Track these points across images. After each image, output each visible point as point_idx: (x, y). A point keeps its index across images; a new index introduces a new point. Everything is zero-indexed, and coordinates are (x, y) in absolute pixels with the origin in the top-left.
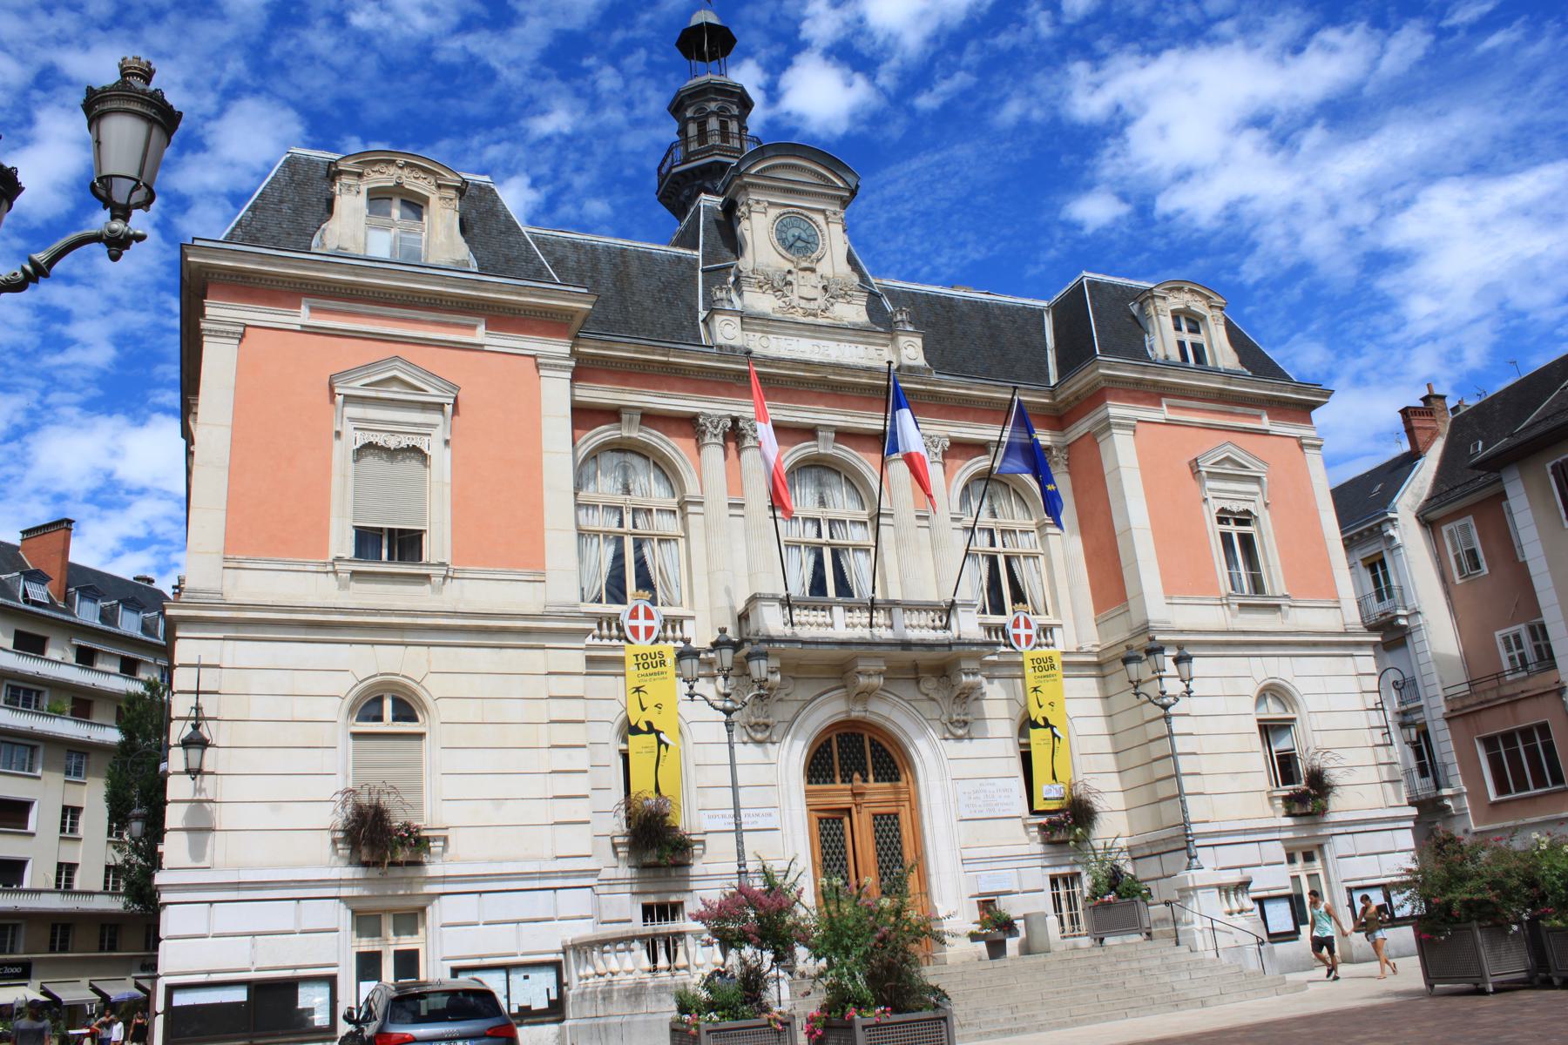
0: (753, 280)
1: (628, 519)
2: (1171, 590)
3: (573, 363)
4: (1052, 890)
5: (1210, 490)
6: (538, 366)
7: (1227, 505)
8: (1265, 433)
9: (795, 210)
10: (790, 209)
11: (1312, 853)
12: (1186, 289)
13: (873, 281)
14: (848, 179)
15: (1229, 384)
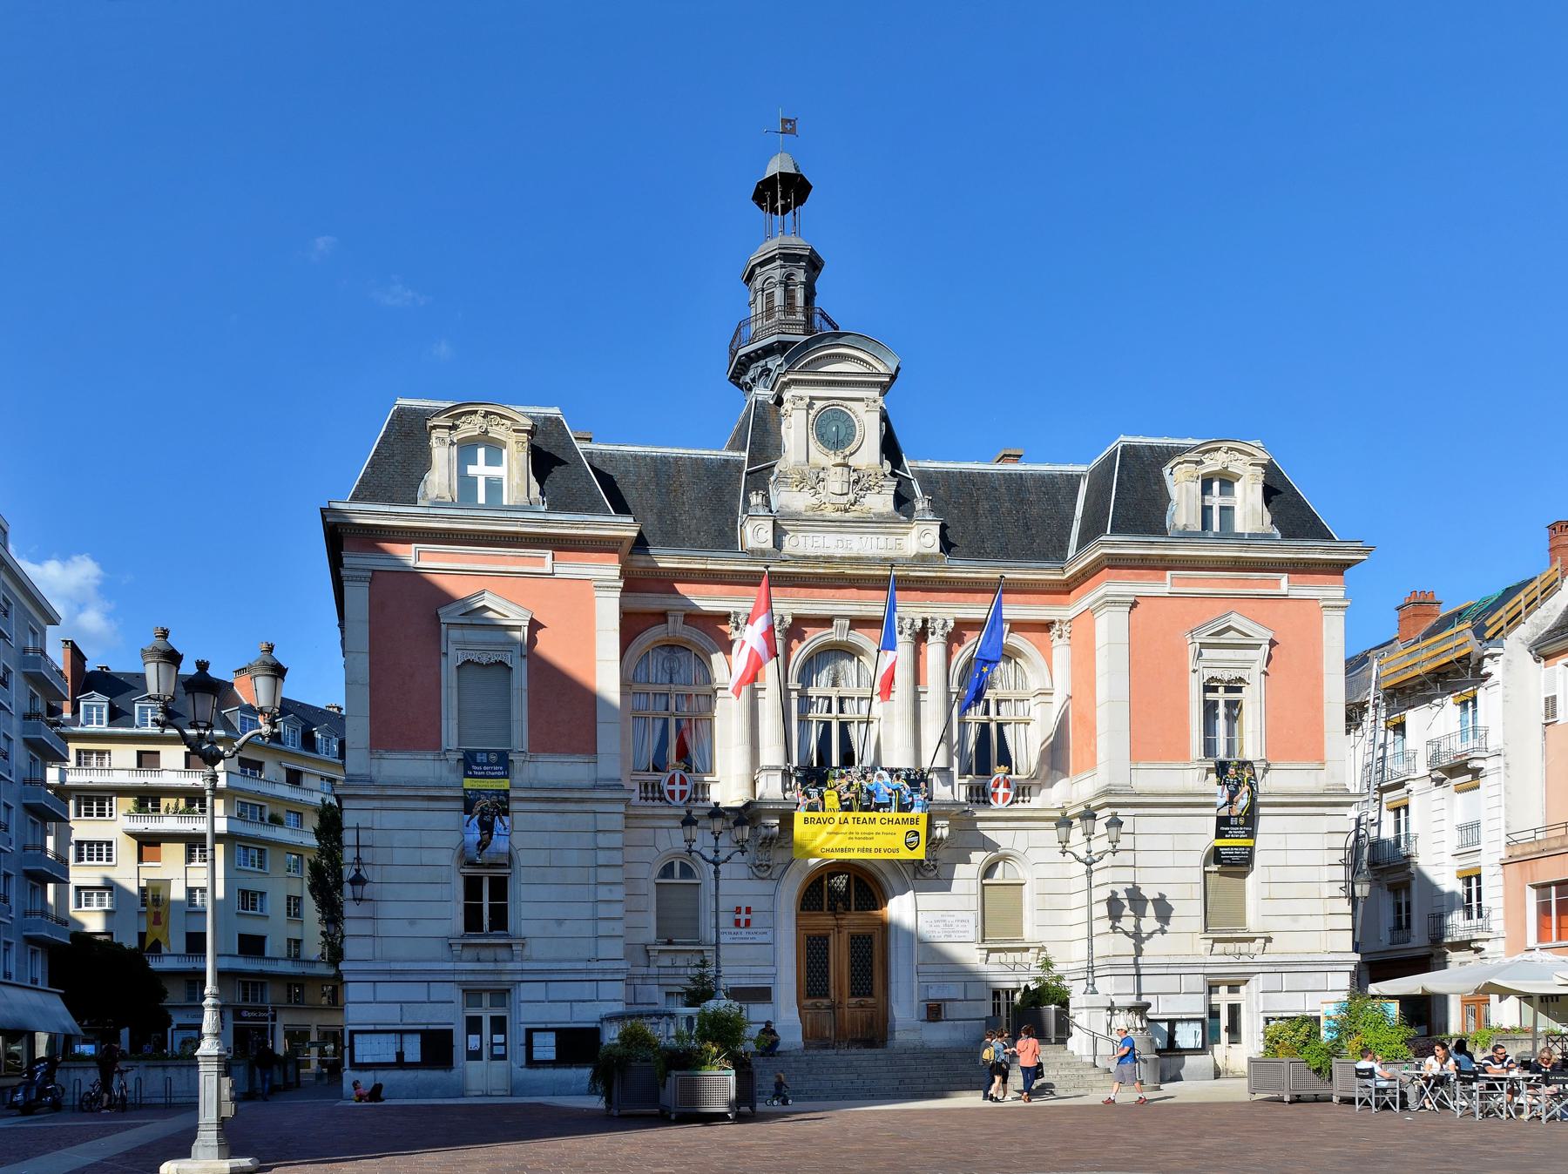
0: (790, 480)
3: (621, 584)
4: (994, 1000)
7: (1217, 674)
8: (1284, 597)
9: (835, 402)
14: (889, 364)
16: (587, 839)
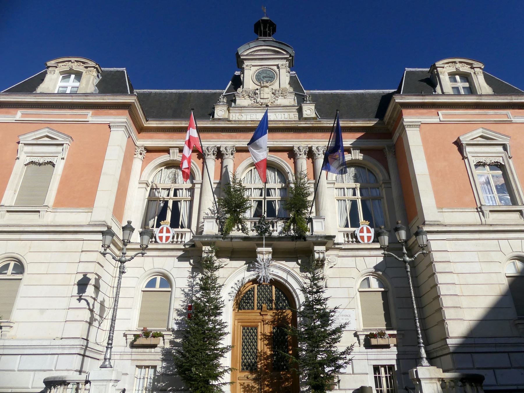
1: (172, 193)
2: (440, 205)
5: (469, 152)
6: (110, 127)
10: (263, 67)
13: (305, 91)
16: (76, 257)
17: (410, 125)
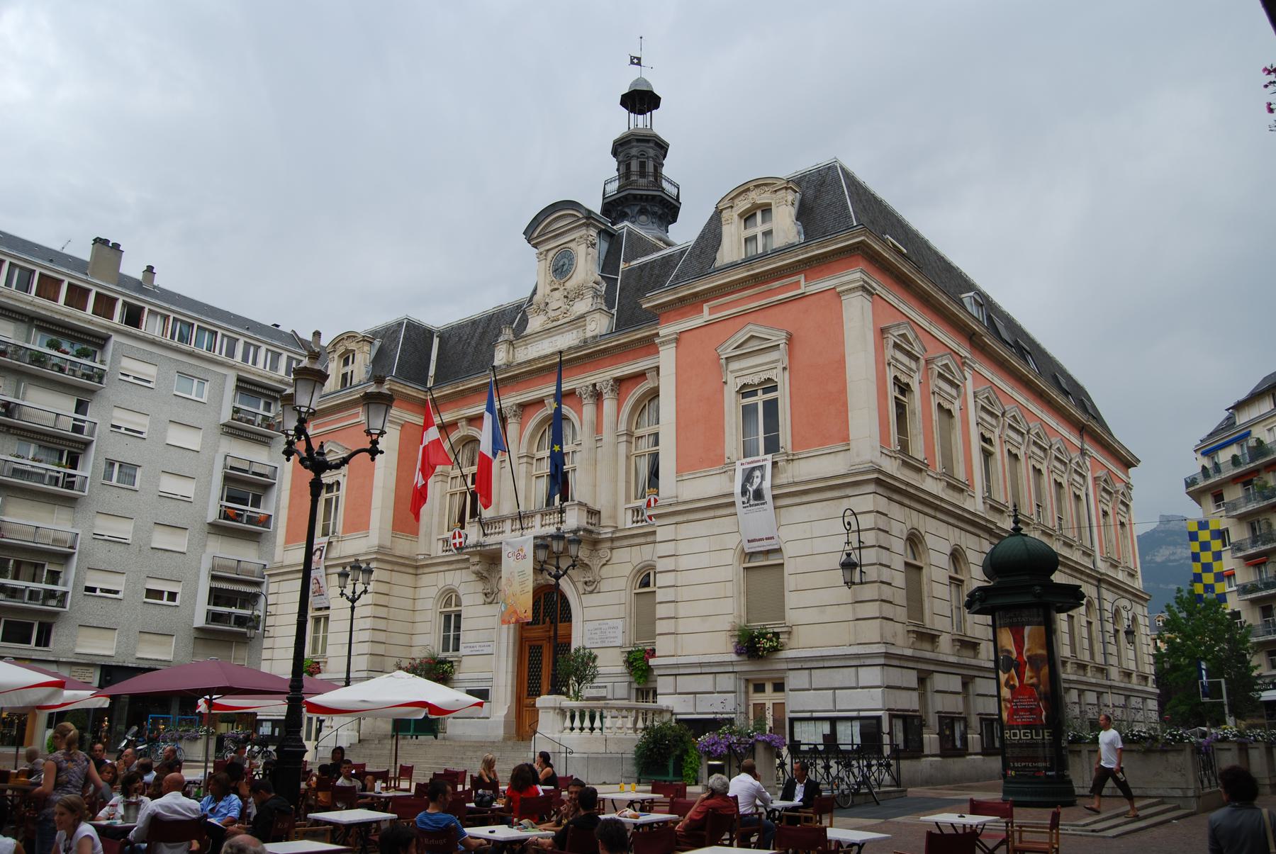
7: (748, 380)
9: (562, 247)
11: (764, 685)
12: (752, 188)
15: (753, 269)
17: (663, 342)
